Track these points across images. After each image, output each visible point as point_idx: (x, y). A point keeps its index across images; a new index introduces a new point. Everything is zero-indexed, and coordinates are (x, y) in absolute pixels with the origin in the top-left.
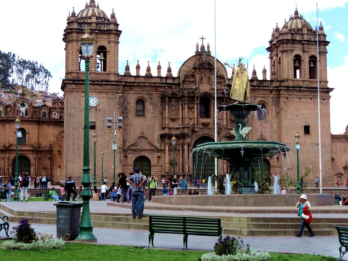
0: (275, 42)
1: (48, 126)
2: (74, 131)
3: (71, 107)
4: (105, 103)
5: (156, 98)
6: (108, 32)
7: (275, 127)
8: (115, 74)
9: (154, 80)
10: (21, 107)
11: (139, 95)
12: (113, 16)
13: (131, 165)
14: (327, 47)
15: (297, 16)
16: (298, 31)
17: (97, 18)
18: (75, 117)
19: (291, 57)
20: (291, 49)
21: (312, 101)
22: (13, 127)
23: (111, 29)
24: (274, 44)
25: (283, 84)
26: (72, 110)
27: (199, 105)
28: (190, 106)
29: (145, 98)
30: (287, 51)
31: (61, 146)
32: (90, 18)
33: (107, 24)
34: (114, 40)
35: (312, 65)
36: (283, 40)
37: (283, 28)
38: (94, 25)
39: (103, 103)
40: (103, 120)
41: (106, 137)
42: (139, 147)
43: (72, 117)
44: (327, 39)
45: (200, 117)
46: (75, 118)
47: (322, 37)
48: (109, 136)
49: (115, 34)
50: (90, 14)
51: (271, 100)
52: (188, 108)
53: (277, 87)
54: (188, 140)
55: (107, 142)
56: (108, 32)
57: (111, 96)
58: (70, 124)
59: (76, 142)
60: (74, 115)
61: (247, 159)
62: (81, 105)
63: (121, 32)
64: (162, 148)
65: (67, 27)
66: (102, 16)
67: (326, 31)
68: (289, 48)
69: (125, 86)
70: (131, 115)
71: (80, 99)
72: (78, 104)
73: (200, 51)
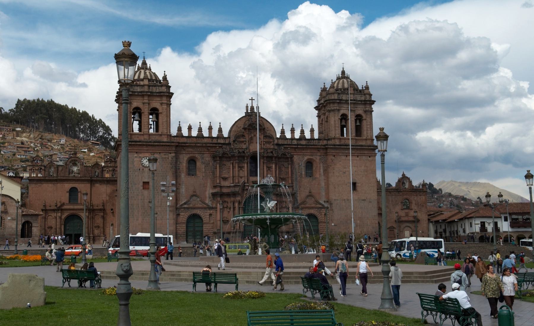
0: (322, 102)
1: (101, 185)
5: (207, 157)
6: (160, 95)
7: (323, 184)
8: (168, 135)
9: (205, 141)
11: (191, 155)
12: (165, 78)
13: (184, 223)
14: (373, 106)
15: (344, 75)
16: (344, 91)
17: (149, 80)
19: (338, 117)
20: (338, 108)
21: (358, 159)
23: (163, 91)
24: (322, 103)
25: (330, 142)
27: (249, 164)
28: (241, 165)
29: (197, 158)
30: (333, 110)
31: (113, 205)
32: (142, 80)
33: (159, 86)
34: (166, 101)
35: (358, 124)
36: (329, 100)
37: (330, 88)
38: (146, 87)
42: (191, 206)
44: (373, 98)
45: (251, 176)
47: (368, 96)
49: (167, 96)
50: (142, 76)
51: (318, 158)
52: (239, 167)
53: (325, 145)
54: (238, 198)
56: (160, 95)
57: (164, 156)
61: (273, 227)
63: (172, 94)
64: (214, 206)
65: (119, 89)
66: (154, 78)
67: (371, 91)
68: (335, 108)
69: (177, 146)
70: (183, 175)
73: (249, 111)
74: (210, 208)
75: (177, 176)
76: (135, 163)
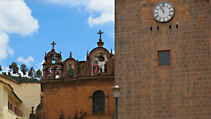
2: (130, 70)
3: (124, 28)
4: (186, 12)
10: (99, 62)
18: (131, 44)
22: (87, 89)
26: (126, 33)
39: (184, 12)
40: (184, 46)
41: (190, 77)
43: (125, 46)
46: (130, 47)
48: (197, 74)
55: (191, 87)
58: (122, 58)
59: (132, 91)
60: (129, 42)
62: (140, 22)
71: (139, 11)
72: (135, 20)
76: (142, 17)
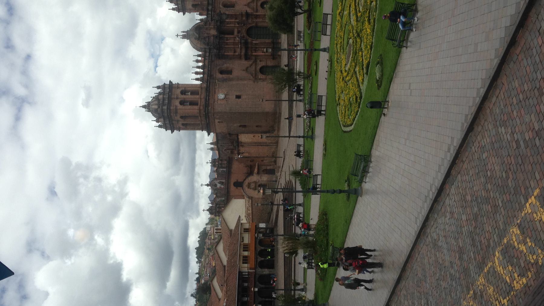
12: (158, 87)
74: (255, 61)
75: (231, 80)
